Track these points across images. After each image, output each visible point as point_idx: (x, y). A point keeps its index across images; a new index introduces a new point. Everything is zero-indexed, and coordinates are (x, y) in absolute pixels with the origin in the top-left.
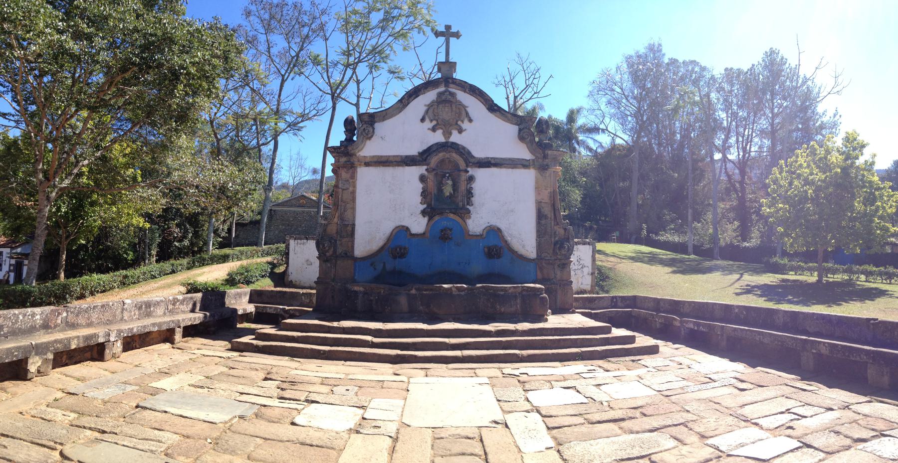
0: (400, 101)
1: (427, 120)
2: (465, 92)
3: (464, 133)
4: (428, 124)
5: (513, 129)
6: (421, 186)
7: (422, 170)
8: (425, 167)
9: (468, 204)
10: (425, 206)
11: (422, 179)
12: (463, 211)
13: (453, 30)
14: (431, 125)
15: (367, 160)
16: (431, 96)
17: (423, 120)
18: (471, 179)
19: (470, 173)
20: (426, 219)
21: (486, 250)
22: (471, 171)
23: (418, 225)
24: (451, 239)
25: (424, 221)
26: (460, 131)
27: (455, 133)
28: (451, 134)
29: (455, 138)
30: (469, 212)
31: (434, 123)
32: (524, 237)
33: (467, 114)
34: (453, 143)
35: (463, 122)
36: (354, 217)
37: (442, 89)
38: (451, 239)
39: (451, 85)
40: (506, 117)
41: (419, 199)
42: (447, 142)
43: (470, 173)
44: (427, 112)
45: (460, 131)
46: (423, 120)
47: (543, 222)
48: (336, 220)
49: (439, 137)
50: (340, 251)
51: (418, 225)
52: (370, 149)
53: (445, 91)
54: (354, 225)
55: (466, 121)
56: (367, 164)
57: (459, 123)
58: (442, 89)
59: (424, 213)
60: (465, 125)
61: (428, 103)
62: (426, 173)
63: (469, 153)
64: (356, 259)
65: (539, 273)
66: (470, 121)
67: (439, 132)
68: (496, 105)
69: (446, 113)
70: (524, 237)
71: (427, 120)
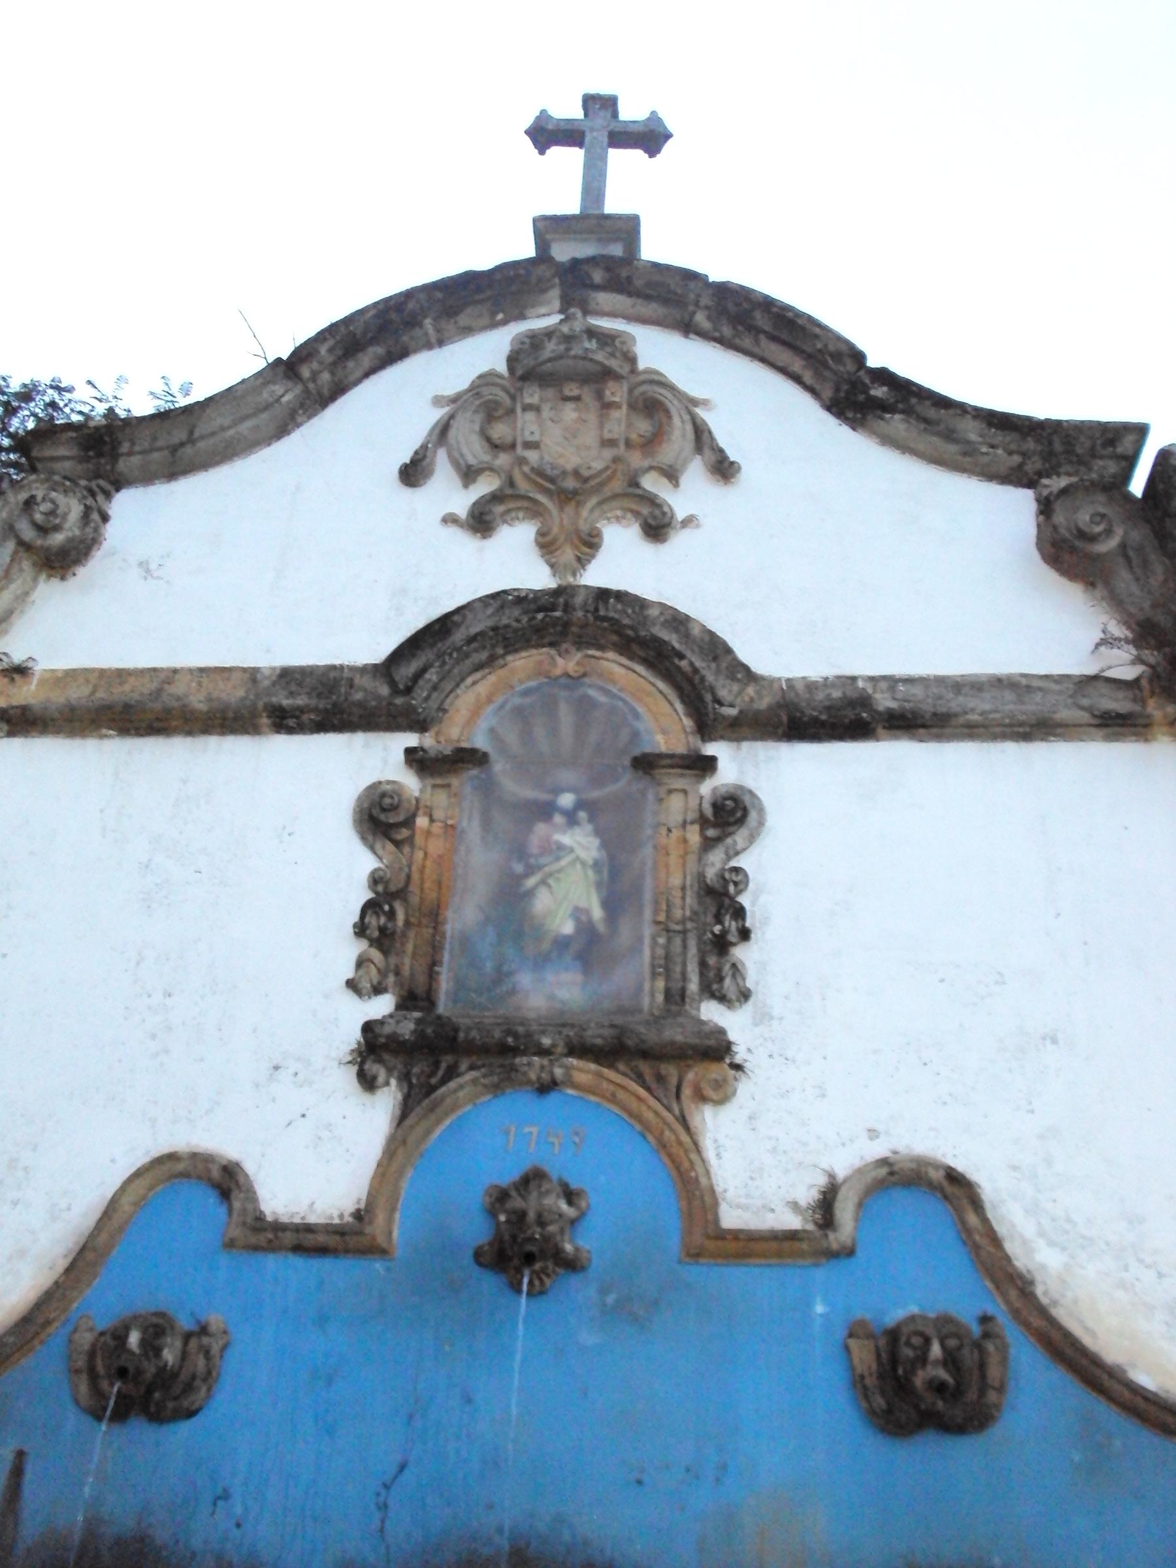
0: (285, 369)
1: (443, 472)
2: (687, 328)
3: (679, 541)
4: (447, 494)
7: (376, 758)
9: (713, 990)
11: (379, 817)
12: (668, 1058)
13: (631, 112)
14: (462, 501)
16: (484, 352)
18: (731, 814)
21: (864, 1356)
22: (735, 764)
23: (319, 1148)
24: (573, 1265)
25: (367, 1121)
26: (657, 528)
28: (590, 544)
29: (621, 562)
33: (701, 436)
34: (603, 594)
35: (672, 475)
38: (573, 1265)
39: (604, 299)
40: (949, 436)
41: (345, 953)
44: (442, 431)
46: (413, 473)
51: (319, 1148)
55: (695, 474)
57: (651, 483)
59: (374, 1051)
60: (693, 494)
62: (411, 783)
63: (716, 648)
66: (724, 469)
68: (884, 376)
69: (563, 435)
71: (443, 472)
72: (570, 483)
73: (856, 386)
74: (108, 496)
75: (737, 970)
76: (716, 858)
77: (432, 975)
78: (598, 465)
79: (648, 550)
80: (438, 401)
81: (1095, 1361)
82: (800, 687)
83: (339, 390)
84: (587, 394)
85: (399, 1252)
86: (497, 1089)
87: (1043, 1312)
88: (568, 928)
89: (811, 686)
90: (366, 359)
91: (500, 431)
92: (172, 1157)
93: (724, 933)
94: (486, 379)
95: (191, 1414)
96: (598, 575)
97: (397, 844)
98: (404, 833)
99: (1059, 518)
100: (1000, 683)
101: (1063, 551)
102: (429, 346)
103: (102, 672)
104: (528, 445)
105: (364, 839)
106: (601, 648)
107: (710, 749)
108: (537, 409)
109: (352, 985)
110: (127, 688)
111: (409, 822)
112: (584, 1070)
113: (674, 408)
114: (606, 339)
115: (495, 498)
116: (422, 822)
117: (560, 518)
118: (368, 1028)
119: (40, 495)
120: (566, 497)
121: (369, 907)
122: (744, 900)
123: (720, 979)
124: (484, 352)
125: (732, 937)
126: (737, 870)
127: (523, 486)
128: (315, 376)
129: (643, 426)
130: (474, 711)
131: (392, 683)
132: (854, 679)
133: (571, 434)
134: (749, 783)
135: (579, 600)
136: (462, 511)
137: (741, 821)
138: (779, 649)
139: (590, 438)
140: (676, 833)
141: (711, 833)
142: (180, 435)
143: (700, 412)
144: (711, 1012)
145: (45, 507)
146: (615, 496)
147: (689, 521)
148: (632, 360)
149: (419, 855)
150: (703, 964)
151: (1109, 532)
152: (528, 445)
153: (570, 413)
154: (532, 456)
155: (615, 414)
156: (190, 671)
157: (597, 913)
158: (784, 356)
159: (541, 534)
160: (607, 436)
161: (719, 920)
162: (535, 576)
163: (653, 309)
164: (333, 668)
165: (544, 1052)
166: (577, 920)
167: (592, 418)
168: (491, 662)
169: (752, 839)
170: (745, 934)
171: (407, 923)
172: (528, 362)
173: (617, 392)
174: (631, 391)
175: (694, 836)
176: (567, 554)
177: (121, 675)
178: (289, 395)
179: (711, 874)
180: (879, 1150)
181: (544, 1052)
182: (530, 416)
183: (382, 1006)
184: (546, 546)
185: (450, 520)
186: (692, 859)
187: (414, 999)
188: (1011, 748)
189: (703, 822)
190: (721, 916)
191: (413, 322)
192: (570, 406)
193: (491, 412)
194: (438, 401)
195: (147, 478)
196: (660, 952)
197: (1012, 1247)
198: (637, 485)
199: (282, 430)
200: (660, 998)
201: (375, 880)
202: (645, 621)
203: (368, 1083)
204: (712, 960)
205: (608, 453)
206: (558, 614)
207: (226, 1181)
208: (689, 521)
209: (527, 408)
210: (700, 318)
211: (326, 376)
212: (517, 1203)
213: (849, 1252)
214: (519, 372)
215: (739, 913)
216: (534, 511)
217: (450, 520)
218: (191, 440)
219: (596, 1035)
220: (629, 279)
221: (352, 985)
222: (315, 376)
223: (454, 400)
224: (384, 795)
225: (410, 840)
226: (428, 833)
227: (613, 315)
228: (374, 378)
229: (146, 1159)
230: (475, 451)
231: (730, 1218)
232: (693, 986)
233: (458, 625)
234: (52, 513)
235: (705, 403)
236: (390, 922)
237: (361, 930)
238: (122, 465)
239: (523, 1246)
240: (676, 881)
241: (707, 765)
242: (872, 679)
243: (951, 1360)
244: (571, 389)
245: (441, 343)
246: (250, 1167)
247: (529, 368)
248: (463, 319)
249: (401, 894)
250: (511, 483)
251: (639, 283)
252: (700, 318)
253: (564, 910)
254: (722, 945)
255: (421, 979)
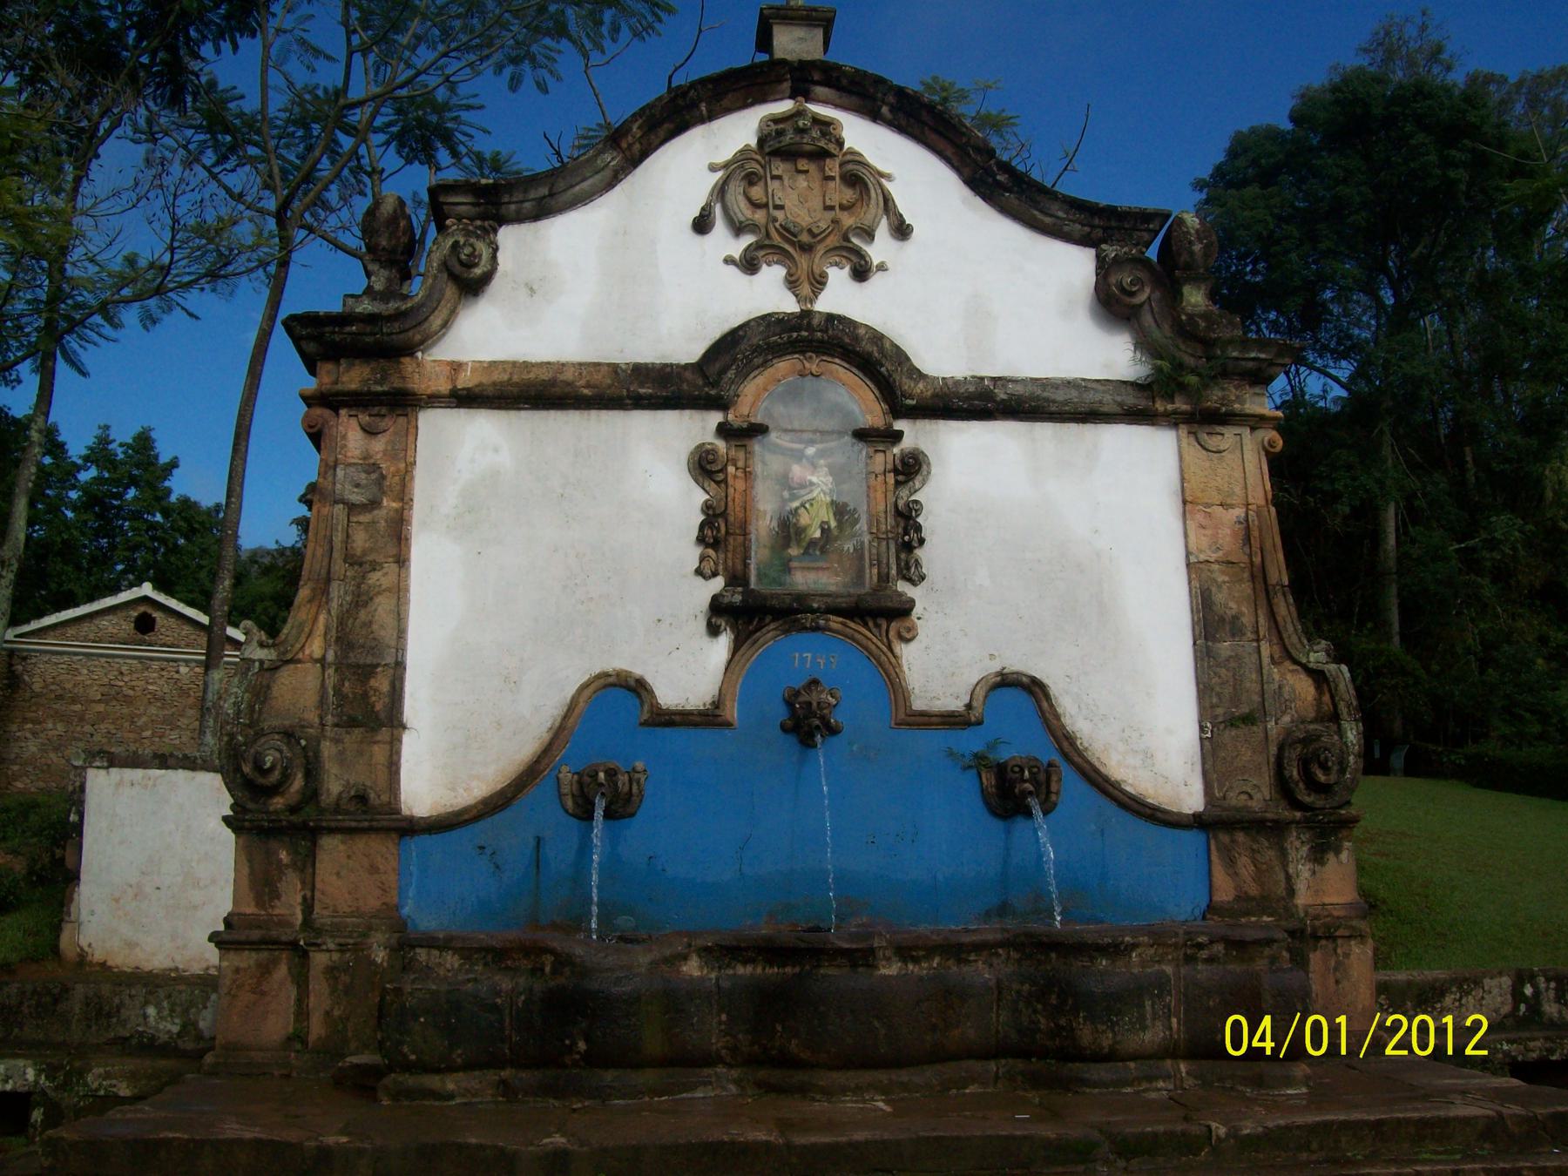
2: (875, 117)
3: (876, 280)
5: (1073, 267)
6: (700, 497)
7: (698, 427)
8: (716, 418)
10: (718, 584)
11: (704, 466)
12: (881, 613)
14: (738, 247)
15: (466, 380)
17: (702, 225)
18: (911, 468)
19: (907, 443)
20: (724, 642)
22: (914, 434)
26: (861, 272)
27: (838, 277)
28: (819, 282)
29: (839, 296)
30: (903, 610)
31: (748, 240)
32: (1148, 721)
33: (888, 201)
34: (830, 318)
35: (869, 235)
36: (401, 633)
37: (784, 106)
38: (833, 731)
39: (820, 90)
41: (691, 554)
42: (806, 314)
43: (907, 443)
44: (720, 191)
45: (861, 272)
46: (702, 225)
47: (1225, 647)
48: (316, 647)
49: (769, 293)
50: (333, 786)
52: (480, 336)
53: (799, 114)
54: (400, 666)
56: (466, 400)
57: (855, 241)
58: (784, 106)
60: (880, 248)
61: (726, 153)
62: (721, 445)
63: (901, 357)
64: (411, 828)
65: (1220, 875)
66: (902, 231)
67: (772, 275)
69: (799, 197)
70: (1148, 721)
72: (805, 238)
73: (988, 171)
74: (495, 231)
75: (918, 564)
76: (904, 493)
77: (746, 566)
78: (823, 225)
79: (855, 287)
80: (713, 168)
81: (1106, 779)
82: (950, 383)
83: (645, 154)
84: (812, 167)
85: (736, 723)
86: (786, 632)
87: (1079, 753)
88: (818, 534)
89: (957, 383)
90: (662, 133)
91: (757, 192)
92: (606, 675)
93: (911, 541)
94: (743, 155)
95: (632, 815)
96: (826, 303)
97: (718, 483)
98: (721, 476)
99: (1113, 280)
100: (1069, 384)
101: (1112, 304)
102: (702, 120)
103: (514, 364)
104: (781, 207)
105: (697, 481)
106: (833, 356)
107: (899, 425)
108: (779, 178)
109: (699, 572)
110: (532, 376)
111: (723, 470)
112: (835, 622)
113: (870, 181)
114: (825, 125)
115: (758, 246)
116: (731, 469)
117: (803, 261)
118: (715, 598)
119: (462, 241)
120: (807, 249)
121: (702, 526)
122: (920, 520)
123: (908, 568)
124: (738, 131)
125: (915, 544)
126: (916, 502)
127: (777, 239)
128: (630, 146)
129: (848, 195)
130: (755, 396)
131: (705, 377)
132: (982, 379)
133: (803, 200)
134: (923, 447)
135: (815, 322)
136: (737, 256)
137: (917, 472)
138: (939, 356)
139: (816, 203)
140: (881, 478)
141: (901, 478)
142: (544, 191)
143: (883, 181)
144: (902, 586)
145: (467, 250)
146: (835, 248)
147: (882, 267)
148: (840, 143)
149: (731, 490)
150: (898, 558)
151: (1142, 289)
152: (781, 207)
153: (802, 182)
154: (779, 214)
155: (832, 184)
156: (573, 365)
157: (833, 524)
158: (942, 144)
159: (789, 274)
160: (828, 203)
161: (906, 533)
162: (788, 304)
163: (854, 100)
164: (666, 365)
165: (813, 611)
166: (823, 531)
167: (816, 185)
168: (765, 364)
169: (923, 483)
170: (922, 541)
171: (727, 533)
172: (773, 144)
173: (833, 167)
174: (841, 165)
175: (891, 478)
176: (806, 289)
177: (527, 365)
178: (611, 159)
179: (901, 503)
180: (995, 667)
181: (813, 611)
182: (776, 184)
183: (718, 584)
184: (792, 283)
185: (729, 261)
186: (890, 495)
187: (736, 579)
188: (1073, 428)
189: (895, 471)
190: (906, 529)
191: (694, 105)
192: (801, 177)
193: (751, 179)
194: (713, 168)
195: (520, 219)
196: (874, 551)
197: (1066, 721)
198: (849, 241)
199: (610, 185)
200: (875, 579)
201: (707, 508)
202: (856, 338)
203: (713, 631)
204: (903, 556)
205: (830, 215)
206: (805, 334)
207: (637, 688)
208: (882, 267)
209: (774, 177)
210: (885, 110)
211: (637, 146)
212: (804, 698)
213: (979, 723)
214: (767, 150)
215: (918, 528)
216: (783, 256)
217: (729, 261)
218: (551, 195)
219: (843, 603)
220: (838, 79)
221: (699, 572)
222: (630, 146)
223: (726, 166)
224: (708, 452)
225: (725, 481)
226: (735, 477)
227: (825, 102)
228: (668, 145)
229: (587, 677)
230: (743, 211)
231: (918, 704)
232: (894, 572)
233: (743, 338)
234: (472, 255)
235: (889, 177)
236: (719, 532)
237: (701, 540)
238: (503, 210)
239: (806, 723)
240: (881, 507)
241: (897, 436)
242: (995, 380)
243: (1034, 779)
244: (803, 164)
245: (711, 117)
246: (649, 679)
247: (777, 146)
248: (725, 103)
249: (724, 514)
250: (768, 235)
251: (844, 82)
252: (885, 110)
253: (817, 523)
254: (908, 548)
255: (739, 567)
